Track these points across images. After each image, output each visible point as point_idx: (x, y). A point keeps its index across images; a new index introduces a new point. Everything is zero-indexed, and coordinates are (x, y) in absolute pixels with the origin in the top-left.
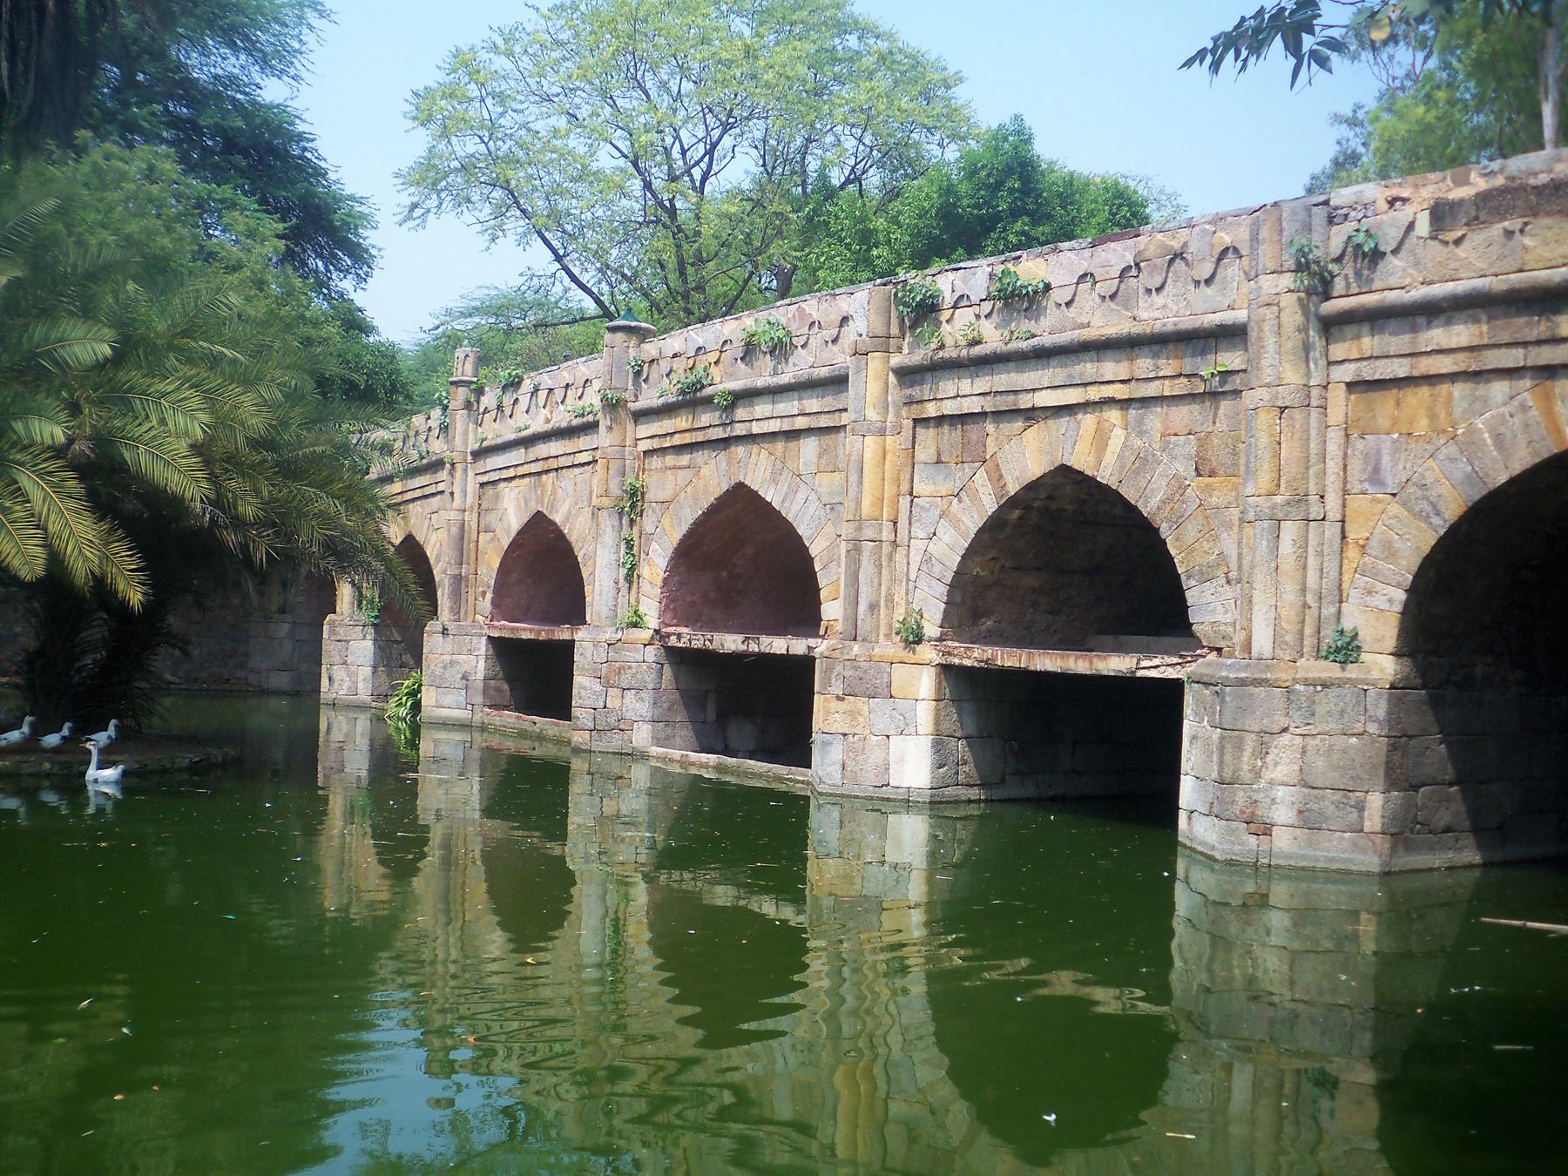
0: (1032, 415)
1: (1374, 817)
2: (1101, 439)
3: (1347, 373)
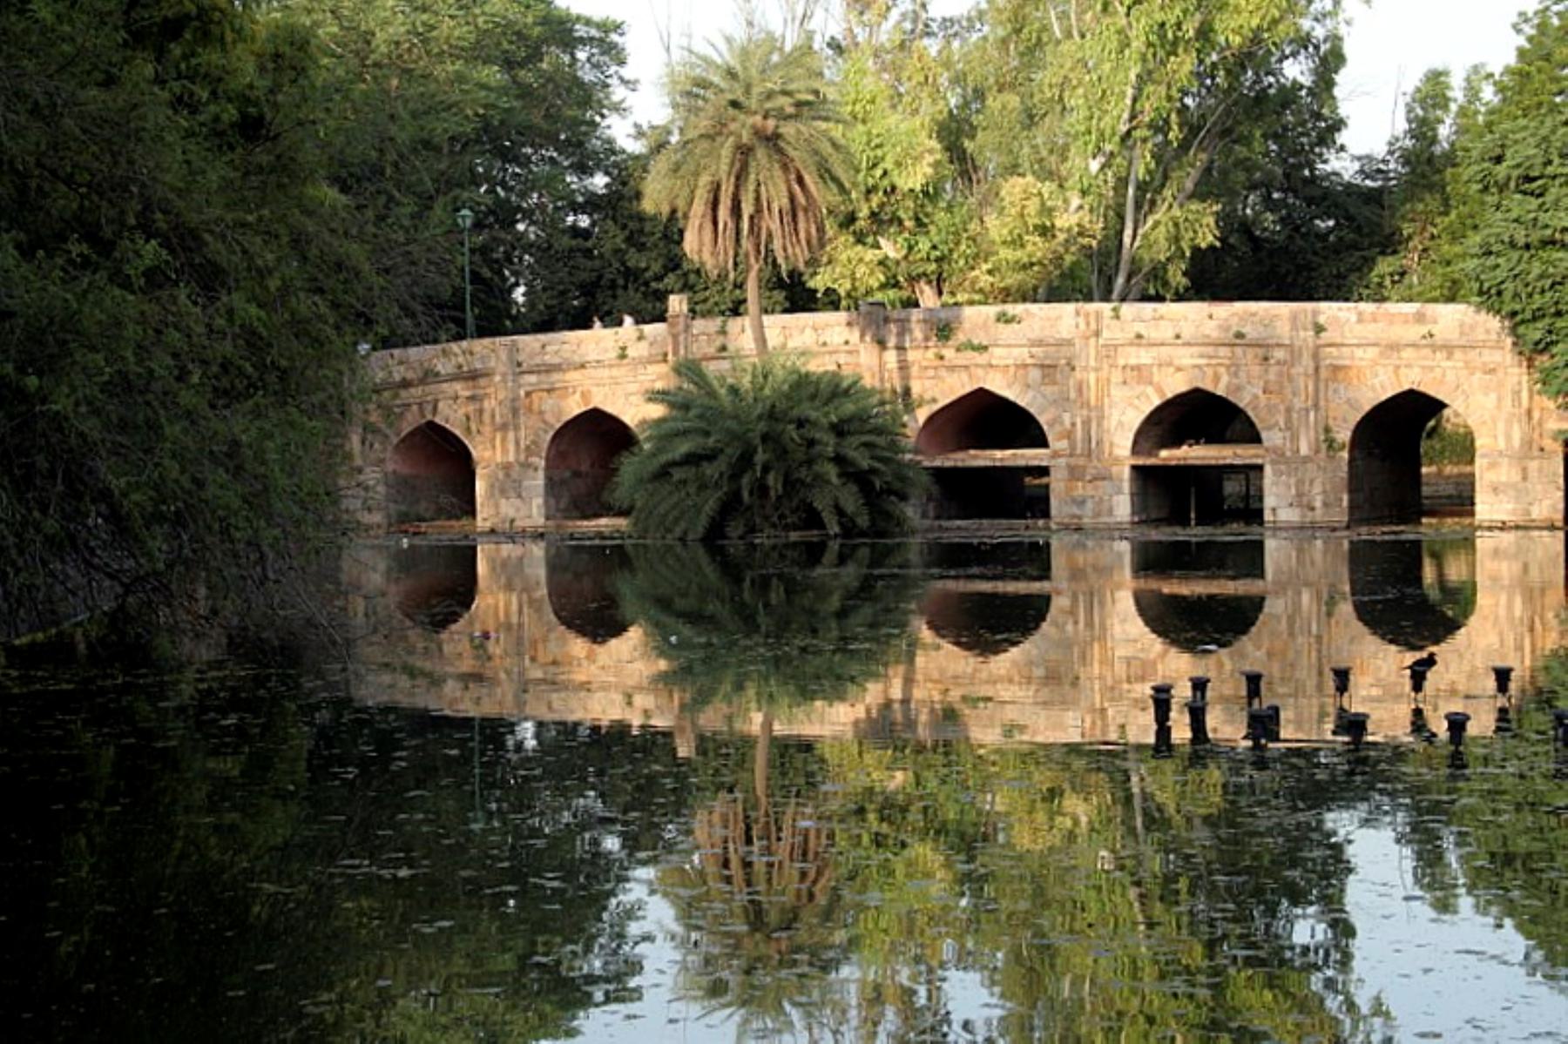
1: (1345, 503)
2: (1217, 379)
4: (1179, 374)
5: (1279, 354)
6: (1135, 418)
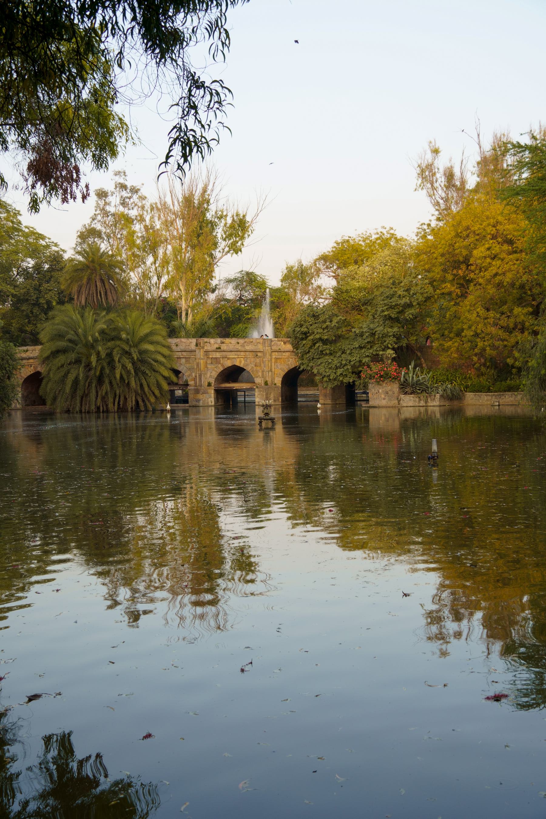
0: (228, 359)
1: (280, 400)
2: (240, 362)
3: (274, 357)
4: (229, 361)
5: (259, 354)
6: (215, 374)
